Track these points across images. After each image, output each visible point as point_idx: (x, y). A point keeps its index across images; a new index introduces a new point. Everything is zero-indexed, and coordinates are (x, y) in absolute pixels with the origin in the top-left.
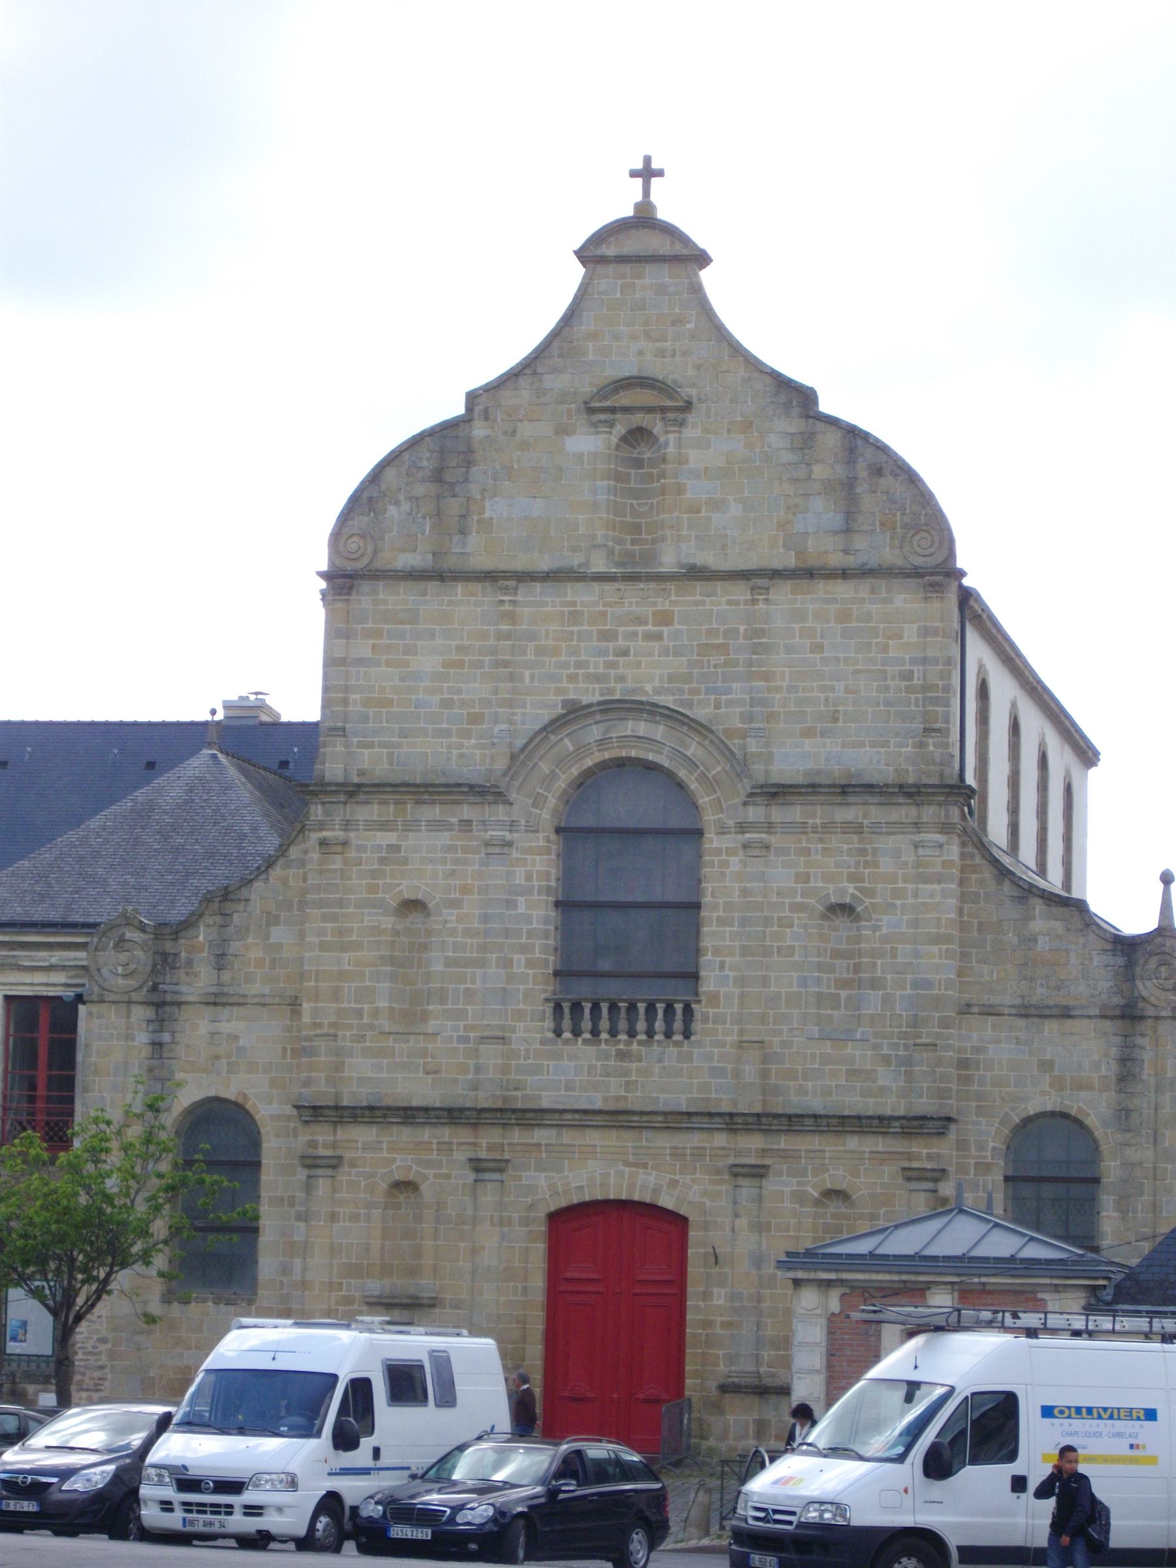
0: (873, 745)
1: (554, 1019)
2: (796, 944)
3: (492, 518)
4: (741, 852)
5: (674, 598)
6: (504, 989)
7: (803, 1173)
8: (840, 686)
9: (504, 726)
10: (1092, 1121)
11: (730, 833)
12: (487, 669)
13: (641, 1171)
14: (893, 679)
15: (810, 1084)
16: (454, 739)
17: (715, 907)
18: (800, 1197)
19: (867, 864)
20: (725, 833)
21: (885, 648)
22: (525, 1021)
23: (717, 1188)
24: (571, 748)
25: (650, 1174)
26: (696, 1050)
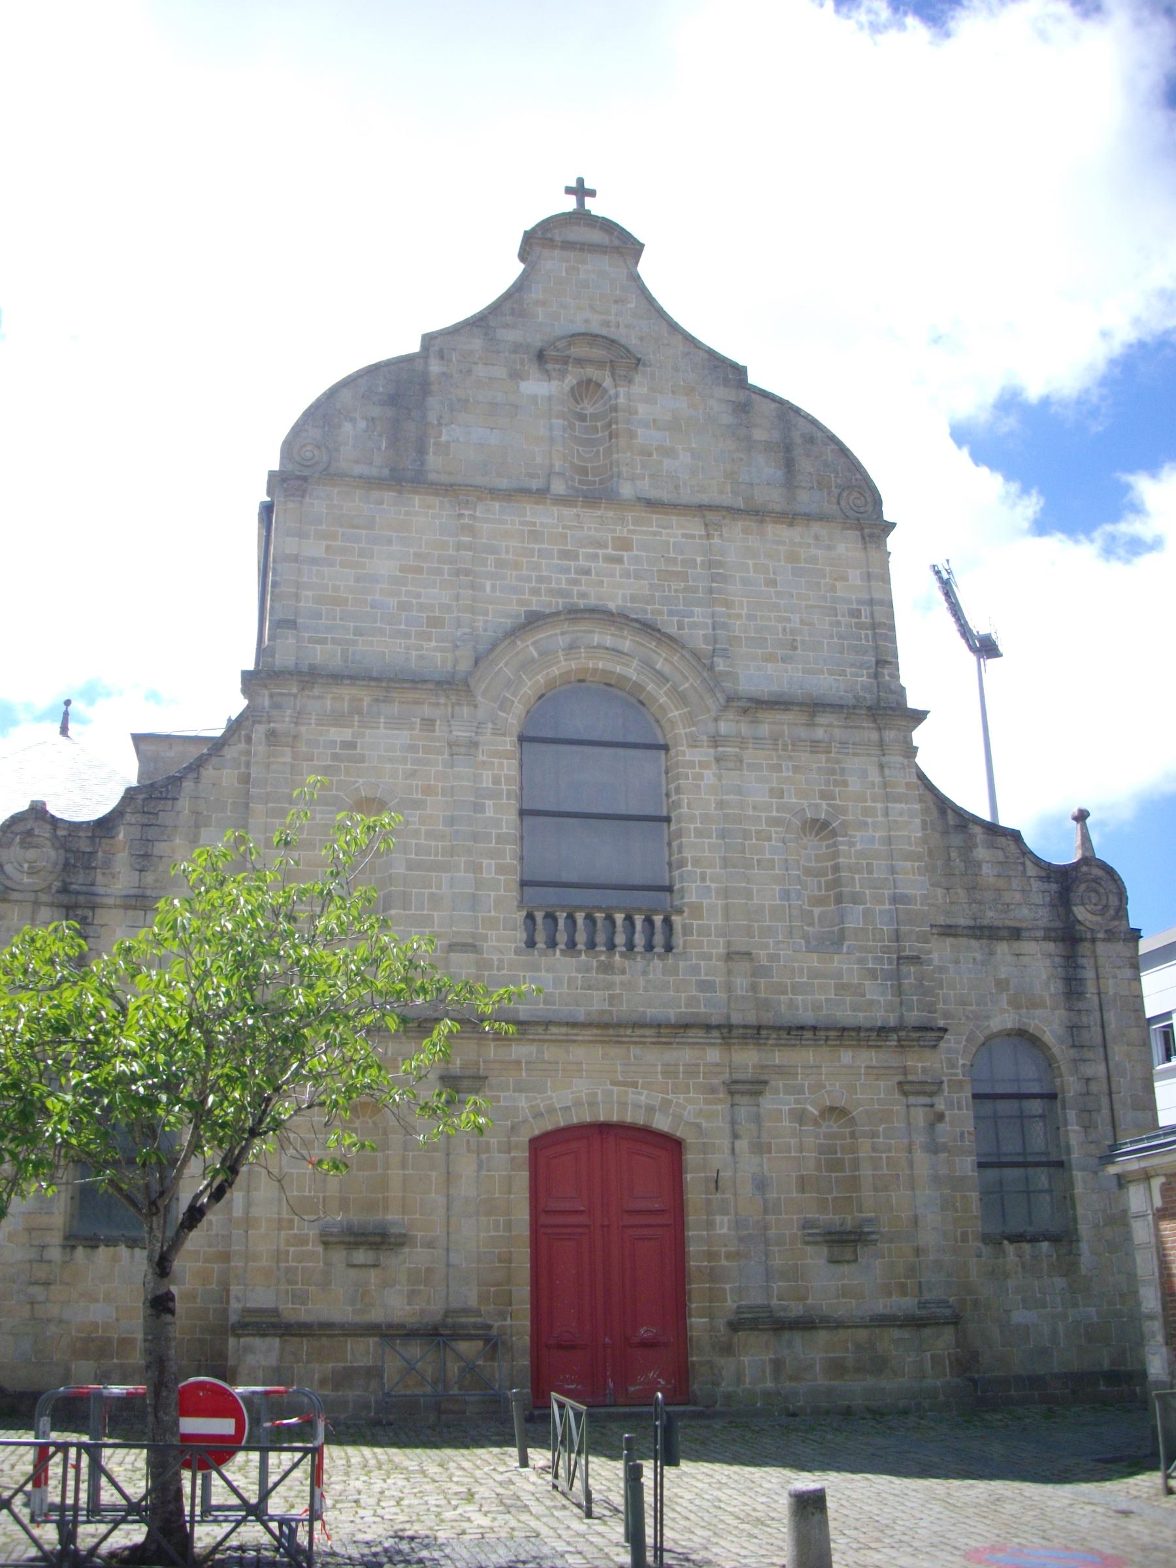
0: (831, 673)
1: (526, 929)
2: (776, 857)
3: (448, 442)
4: (714, 766)
5: (631, 527)
6: (474, 895)
7: (800, 1091)
8: (796, 618)
9: (467, 630)
10: (1048, 1038)
11: (702, 746)
12: (446, 577)
13: (630, 1090)
14: (843, 616)
15: (800, 998)
16: (413, 641)
17: (692, 819)
18: (800, 1117)
19: (836, 783)
20: (696, 746)
21: (833, 589)
22: (498, 929)
23: (714, 1107)
24: (535, 654)
25: (640, 1094)
26: (681, 964)
